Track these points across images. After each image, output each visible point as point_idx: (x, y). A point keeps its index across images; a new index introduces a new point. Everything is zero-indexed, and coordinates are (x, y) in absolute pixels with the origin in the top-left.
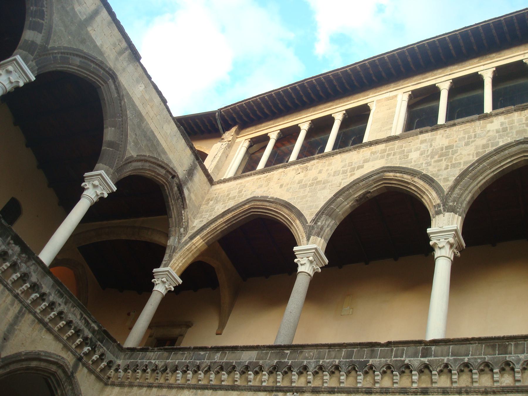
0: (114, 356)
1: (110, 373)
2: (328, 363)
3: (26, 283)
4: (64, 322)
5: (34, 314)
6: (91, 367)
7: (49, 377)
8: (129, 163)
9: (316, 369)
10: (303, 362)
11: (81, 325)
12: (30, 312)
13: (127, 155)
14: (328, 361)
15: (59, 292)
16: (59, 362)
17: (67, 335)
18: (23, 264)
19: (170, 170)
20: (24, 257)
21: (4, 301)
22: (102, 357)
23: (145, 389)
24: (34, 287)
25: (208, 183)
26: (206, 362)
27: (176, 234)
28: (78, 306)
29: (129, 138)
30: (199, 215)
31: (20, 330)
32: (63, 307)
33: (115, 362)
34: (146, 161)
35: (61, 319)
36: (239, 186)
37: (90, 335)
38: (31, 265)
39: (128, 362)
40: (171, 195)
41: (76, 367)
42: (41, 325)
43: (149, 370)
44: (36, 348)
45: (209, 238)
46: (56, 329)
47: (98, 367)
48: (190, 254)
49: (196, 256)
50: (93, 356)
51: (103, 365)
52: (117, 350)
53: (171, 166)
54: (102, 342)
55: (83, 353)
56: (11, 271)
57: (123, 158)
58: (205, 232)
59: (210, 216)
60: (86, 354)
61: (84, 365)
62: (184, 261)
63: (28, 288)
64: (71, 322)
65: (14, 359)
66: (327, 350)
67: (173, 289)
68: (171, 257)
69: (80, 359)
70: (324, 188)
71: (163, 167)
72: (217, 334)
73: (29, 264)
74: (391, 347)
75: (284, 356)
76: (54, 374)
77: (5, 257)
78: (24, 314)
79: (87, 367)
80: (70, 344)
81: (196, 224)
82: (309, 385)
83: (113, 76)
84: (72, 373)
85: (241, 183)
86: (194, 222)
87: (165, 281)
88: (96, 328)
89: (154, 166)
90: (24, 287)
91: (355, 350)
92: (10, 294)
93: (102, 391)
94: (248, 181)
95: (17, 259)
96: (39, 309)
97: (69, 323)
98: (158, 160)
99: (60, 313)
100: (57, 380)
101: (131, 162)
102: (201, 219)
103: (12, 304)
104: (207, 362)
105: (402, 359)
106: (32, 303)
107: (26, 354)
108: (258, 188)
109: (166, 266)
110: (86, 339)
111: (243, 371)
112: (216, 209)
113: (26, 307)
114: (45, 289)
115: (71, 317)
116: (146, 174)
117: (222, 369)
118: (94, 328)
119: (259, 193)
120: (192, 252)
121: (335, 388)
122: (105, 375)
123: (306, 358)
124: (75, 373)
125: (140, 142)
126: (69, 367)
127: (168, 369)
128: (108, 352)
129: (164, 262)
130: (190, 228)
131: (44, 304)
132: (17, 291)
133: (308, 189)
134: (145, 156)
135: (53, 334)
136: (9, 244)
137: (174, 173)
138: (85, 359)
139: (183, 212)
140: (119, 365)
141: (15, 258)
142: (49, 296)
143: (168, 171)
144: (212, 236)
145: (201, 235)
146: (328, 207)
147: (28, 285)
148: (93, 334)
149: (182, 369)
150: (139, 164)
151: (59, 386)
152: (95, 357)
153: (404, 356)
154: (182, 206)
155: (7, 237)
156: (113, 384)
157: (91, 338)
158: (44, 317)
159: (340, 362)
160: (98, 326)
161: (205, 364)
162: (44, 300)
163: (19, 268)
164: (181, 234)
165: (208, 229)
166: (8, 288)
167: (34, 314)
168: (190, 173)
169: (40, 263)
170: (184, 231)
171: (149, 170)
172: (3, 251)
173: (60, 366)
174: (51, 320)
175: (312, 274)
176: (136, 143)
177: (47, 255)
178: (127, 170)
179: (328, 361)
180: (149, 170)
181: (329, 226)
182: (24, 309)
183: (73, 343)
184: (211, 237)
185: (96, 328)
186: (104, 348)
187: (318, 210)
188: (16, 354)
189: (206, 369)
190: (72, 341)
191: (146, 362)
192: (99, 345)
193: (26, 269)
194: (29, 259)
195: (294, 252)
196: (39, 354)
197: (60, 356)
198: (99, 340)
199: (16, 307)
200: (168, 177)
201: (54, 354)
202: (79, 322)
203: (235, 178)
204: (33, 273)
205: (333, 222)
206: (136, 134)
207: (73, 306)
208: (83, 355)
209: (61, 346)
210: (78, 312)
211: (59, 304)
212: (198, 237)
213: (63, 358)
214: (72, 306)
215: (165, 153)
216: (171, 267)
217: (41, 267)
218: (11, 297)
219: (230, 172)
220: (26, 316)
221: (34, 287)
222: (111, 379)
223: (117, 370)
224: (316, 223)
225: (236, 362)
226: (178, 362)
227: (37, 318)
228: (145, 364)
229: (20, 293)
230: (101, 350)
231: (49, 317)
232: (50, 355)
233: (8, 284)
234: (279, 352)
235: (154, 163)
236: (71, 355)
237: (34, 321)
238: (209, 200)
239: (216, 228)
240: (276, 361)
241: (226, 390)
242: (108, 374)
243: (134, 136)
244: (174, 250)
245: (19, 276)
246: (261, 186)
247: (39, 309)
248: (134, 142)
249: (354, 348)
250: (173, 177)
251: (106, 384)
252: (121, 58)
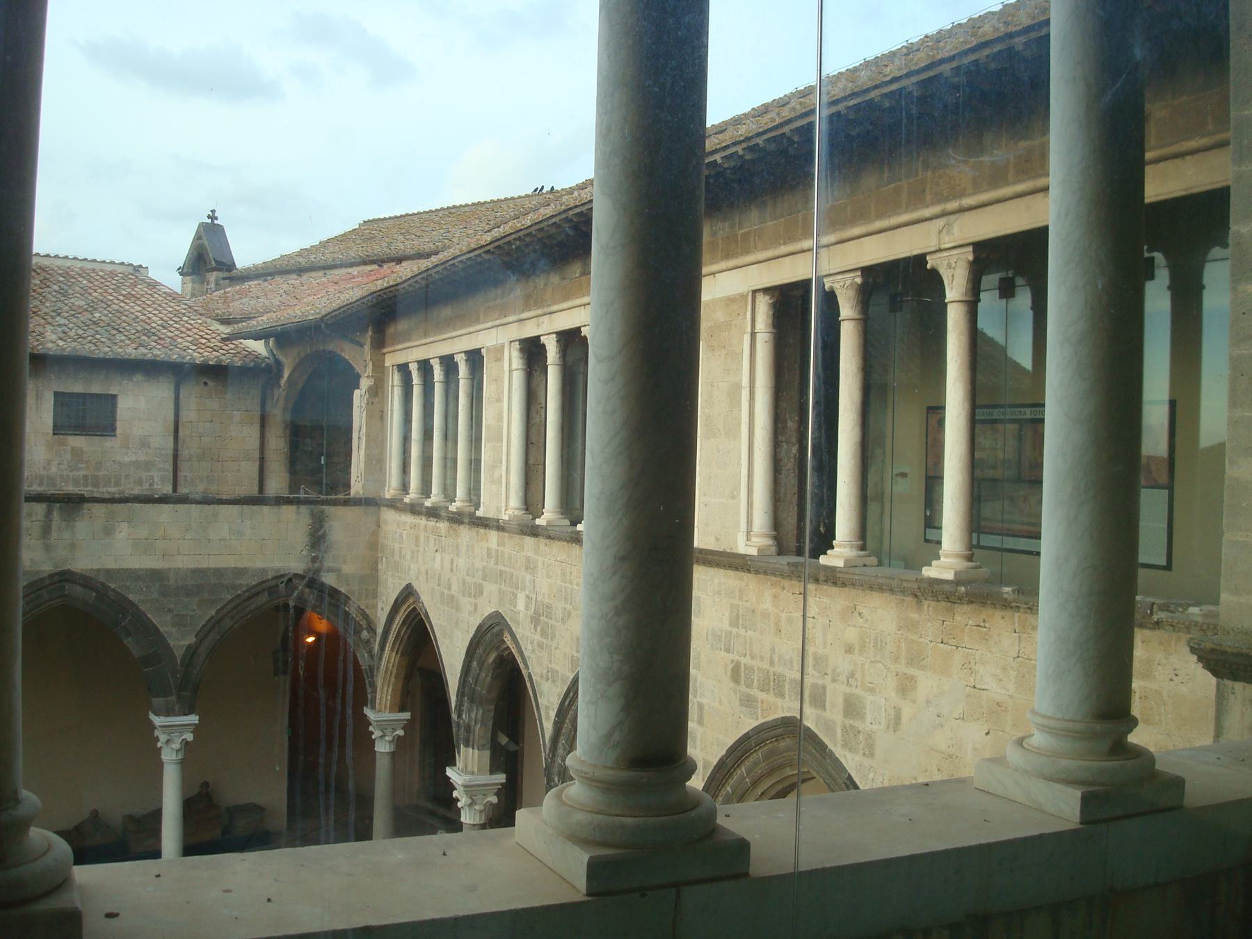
13: (179, 654)
48: (393, 679)
58: (391, 638)
71: (257, 594)
83: (66, 577)
98: (239, 596)
164: (368, 641)
168: (317, 539)
205: (481, 712)
206: (170, 611)
215: (240, 572)
248: (173, 626)
252: (54, 535)
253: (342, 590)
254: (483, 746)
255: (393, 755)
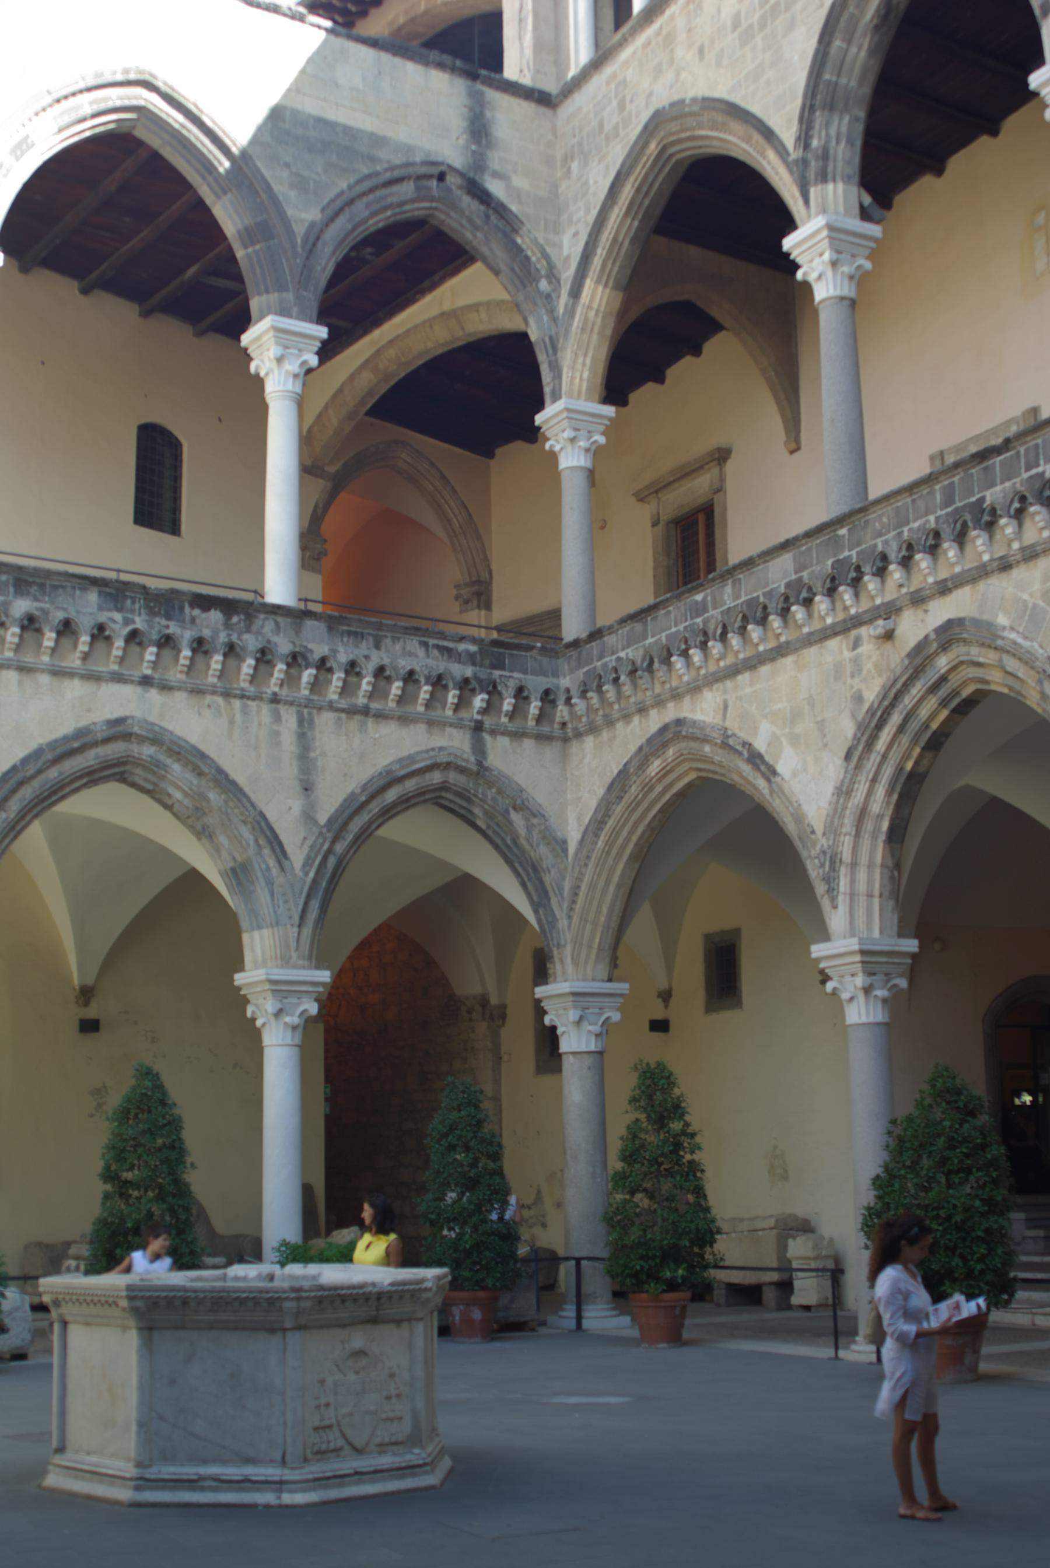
0: (545, 675)
1: (558, 714)
2: (919, 529)
3: (274, 666)
4: (398, 684)
5: (331, 707)
6: (511, 727)
7: (440, 797)
8: (314, 244)
9: (904, 553)
10: (875, 545)
11: (439, 664)
12: (320, 709)
14: (916, 525)
15: (349, 633)
16: (438, 760)
17: (420, 701)
18: (245, 636)
19: (423, 170)
20: (239, 622)
21: (260, 725)
22: (521, 694)
23: (636, 719)
24: (295, 660)
25: (542, 110)
26: (712, 616)
27: (535, 304)
28: (406, 634)
29: (277, 188)
30: (565, 217)
31: (324, 754)
32: (377, 658)
33: (558, 687)
34: (351, 202)
35: (389, 679)
36: (613, 86)
37: (469, 671)
38: (262, 626)
39: (580, 674)
40: (464, 222)
41: (479, 749)
42: (357, 717)
43: (623, 678)
44: (375, 765)
45: (614, 273)
46: (392, 705)
47: (526, 718)
48: (595, 337)
49: (609, 332)
50: (501, 704)
51: (534, 707)
52: (545, 661)
53: (418, 159)
54: (502, 667)
55: (478, 713)
56: (232, 662)
57: (294, 245)
58: (597, 262)
59: (587, 211)
60: (484, 711)
61: (493, 733)
62: (588, 361)
63: (287, 673)
64: (411, 673)
65: (348, 812)
66: (909, 500)
67: (602, 440)
68: (556, 368)
69: (478, 727)
70: (791, 26)
71: (399, 180)
72: (792, 452)
73: (254, 628)
74: (1014, 448)
75: (837, 543)
76: (444, 787)
77: (204, 648)
78: (311, 721)
79: (503, 734)
80: (439, 712)
81: (569, 247)
82: (904, 590)
84: (480, 764)
85: (614, 76)
86: (561, 243)
87: (572, 434)
88: (473, 648)
89: (378, 194)
90: (276, 675)
91: (956, 479)
92: (262, 704)
93: (565, 757)
94: (627, 63)
95: (229, 635)
96: (335, 692)
97: (410, 677)
98: (377, 174)
99: (380, 671)
100: (459, 795)
101: (318, 238)
102: (573, 230)
103: (277, 718)
104: (714, 614)
105: (1040, 469)
106: (312, 691)
107: (364, 787)
108: (655, 79)
109: (556, 397)
110: (464, 685)
111: (783, 609)
112: (591, 182)
113: (306, 707)
114: (319, 649)
115: (405, 664)
116: (373, 229)
117: (745, 619)
118: (467, 651)
119: (663, 95)
120: (596, 329)
121: (945, 580)
122: (552, 722)
123: (880, 534)
124: (485, 758)
125: (306, 173)
126: (465, 756)
127: (656, 660)
128: (529, 677)
129: (547, 390)
130: (559, 265)
131: (335, 677)
132: (269, 691)
133: (758, 40)
134: (343, 192)
135: (392, 718)
136: (193, 620)
137: (435, 171)
138: (488, 722)
139: (519, 240)
140: (568, 690)
141: (222, 637)
142: (335, 657)
143: (419, 178)
144: (618, 264)
145: (591, 274)
146: (816, 85)
147: (281, 666)
148: (474, 664)
149: (678, 649)
150: (342, 223)
151: (469, 800)
152: (508, 704)
153: (1042, 462)
154: (508, 229)
155: (182, 609)
156: (578, 735)
157: (475, 676)
158: (354, 700)
159: (937, 519)
160: (474, 640)
161: (713, 621)
162: (330, 670)
163: (243, 649)
164: (548, 296)
165: (599, 251)
166: (249, 698)
167: (331, 707)
168: (479, 129)
169: (276, 610)
170: (550, 282)
171: (374, 214)
172: (193, 642)
173: (447, 766)
174: (371, 696)
175: (847, 290)
176: (301, 184)
177: (279, 582)
178: (323, 262)
179: (916, 525)
180: (374, 214)
181: (842, 136)
182: (306, 711)
183: (444, 707)
184: (616, 269)
185: (473, 648)
186: (516, 675)
187: (798, 102)
188: (345, 800)
189: (719, 631)
190: (438, 705)
191: (610, 660)
192: (501, 676)
193: (257, 639)
194: (249, 618)
195: (788, 255)
196: (388, 772)
197: (433, 749)
198: (494, 667)
199: (290, 718)
200: (429, 189)
201: (418, 753)
202: (431, 662)
203: (596, 65)
204: (276, 639)
206: (287, 165)
207: (395, 639)
208: (479, 717)
209: (422, 728)
210: (413, 644)
211: (367, 657)
212: (588, 284)
213: (441, 749)
214: (394, 642)
216: (570, 396)
217: (282, 615)
218: (266, 710)
219: (580, 50)
220: (316, 720)
221: (295, 660)
222: (569, 725)
223: (568, 701)
224: (807, 146)
225: (764, 594)
226: (667, 636)
227: (343, 710)
228: (610, 667)
229: (276, 689)
230: (512, 684)
231: (361, 693)
232: (411, 758)
233: (243, 690)
234: (830, 539)
235: (371, 190)
236: (454, 731)
237: (339, 719)
238: (567, 158)
239: (615, 240)
240: (829, 563)
241: (773, 660)
242: (558, 719)
243: (285, 174)
244: (554, 346)
245: (253, 662)
246: (658, 71)
247: (335, 692)
248: (292, 186)
249: (954, 476)
250: (441, 177)
251: (566, 740)
253: (514, 208)
254: (849, 177)
255: (591, 475)
